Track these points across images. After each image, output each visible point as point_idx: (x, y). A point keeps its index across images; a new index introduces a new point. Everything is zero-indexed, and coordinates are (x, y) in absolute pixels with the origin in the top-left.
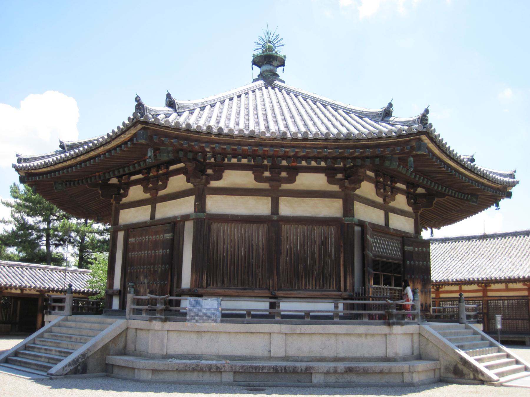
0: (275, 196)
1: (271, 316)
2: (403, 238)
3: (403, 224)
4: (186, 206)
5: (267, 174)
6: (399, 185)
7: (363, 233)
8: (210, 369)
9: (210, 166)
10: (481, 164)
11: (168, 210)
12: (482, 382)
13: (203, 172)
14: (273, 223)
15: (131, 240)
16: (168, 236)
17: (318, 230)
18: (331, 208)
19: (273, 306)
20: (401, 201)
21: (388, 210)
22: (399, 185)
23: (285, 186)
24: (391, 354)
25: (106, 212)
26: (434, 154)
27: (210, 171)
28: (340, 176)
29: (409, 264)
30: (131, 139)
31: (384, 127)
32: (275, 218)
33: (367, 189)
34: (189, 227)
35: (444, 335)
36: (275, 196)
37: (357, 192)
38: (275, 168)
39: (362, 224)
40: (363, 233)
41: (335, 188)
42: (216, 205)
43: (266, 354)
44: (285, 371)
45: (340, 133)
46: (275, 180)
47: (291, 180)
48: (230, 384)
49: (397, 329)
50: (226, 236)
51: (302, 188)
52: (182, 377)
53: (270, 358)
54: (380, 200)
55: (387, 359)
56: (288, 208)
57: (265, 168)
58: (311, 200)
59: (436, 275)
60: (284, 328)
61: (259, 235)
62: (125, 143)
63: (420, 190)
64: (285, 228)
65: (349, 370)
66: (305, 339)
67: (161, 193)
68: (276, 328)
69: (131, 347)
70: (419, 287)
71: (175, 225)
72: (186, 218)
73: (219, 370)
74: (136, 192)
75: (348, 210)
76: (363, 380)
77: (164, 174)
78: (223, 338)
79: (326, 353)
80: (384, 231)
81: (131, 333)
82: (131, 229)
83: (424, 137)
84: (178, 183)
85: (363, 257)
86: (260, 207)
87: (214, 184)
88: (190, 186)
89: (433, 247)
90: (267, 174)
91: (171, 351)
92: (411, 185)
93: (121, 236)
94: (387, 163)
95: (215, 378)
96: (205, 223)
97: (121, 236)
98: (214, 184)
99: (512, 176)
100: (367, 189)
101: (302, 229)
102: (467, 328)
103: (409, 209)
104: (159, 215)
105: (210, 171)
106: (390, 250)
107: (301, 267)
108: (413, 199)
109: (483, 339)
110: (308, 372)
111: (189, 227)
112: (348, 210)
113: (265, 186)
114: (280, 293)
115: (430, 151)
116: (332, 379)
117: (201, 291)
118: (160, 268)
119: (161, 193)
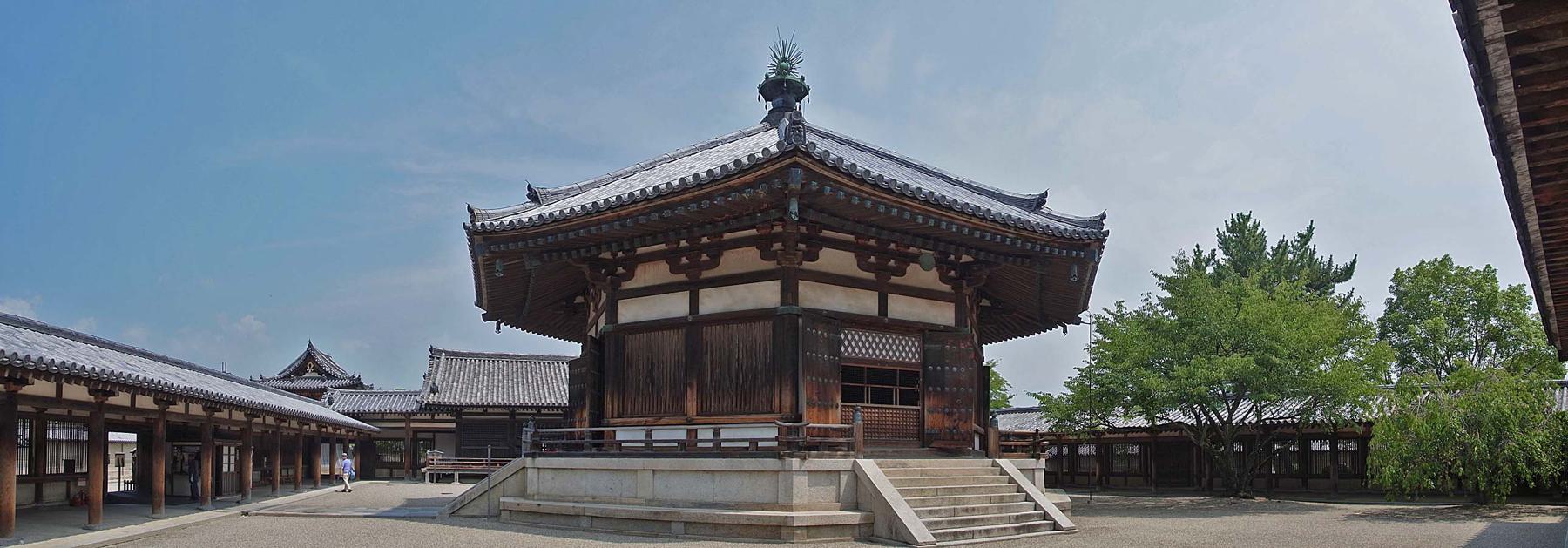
0: (693, 287)
1: (687, 449)
14: (694, 325)
18: (766, 295)
21: (885, 293)
23: (706, 274)
28: (777, 246)
36: (693, 287)
41: (770, 265)
46: (697, 266)
47: (714, 262)
54: (870, 276)
56: (714, 301)
80: (880, 324)
101: (738, 330)
103: (947, 288)
113: (682, 277)
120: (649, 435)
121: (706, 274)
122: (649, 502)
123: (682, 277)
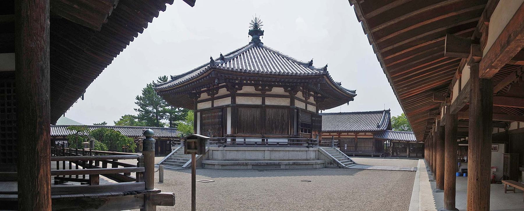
0: (263, 97)
2: (312, 114)
3: (311, 108)
4: (227, 101)
5: (260, 87)
6: (311, 93)
7: (298, 112)
8: (243, 165)
9: (237, 84)
10: (343, 86)
11: (219, 103)
12: (340, 168)
13: (234, 87)
14: (263, 107)
15: (204, 116)
16: (220, 113)
17: (280, 111)
18: (285, 102)
19: (263, 140)
20: (312, 99)
21: (307, 103)
22: (311, 93)
23: (268, 93)
24: (308, 158)
25: (191, 105)
26: (328, 83)
27: (237, 87)
28: (289, 89)
29: (314, 124)
30: (208, 75)
31: (309, 71)
32: (264, 106)
33: (299, 94)
34: (229, 110)
35: (327, 151)
36: (263, 97)
37: (296, 96)
38: (263, 86)
39: (297, 109)
40: (298, 112)
41: (287, 94)
42: (240, 101)
43: (263, 158)
44: (271, 165)
45: (293, 73)
48: (251, 169)
49: (311, 149)
50: (245, 114)
51: (274, 93)
52: (232, 167)
53: (264, 160)
54: (304, 99)
55: (307, 160)
57: (260, 85)
58: (278, 99)
59: (323, 129)
60: (270, 148)
61: (257, 113)
62: (206, 77)
63: (319, 95)
64: (268, 110)
65: (294, 164)
66: (277, 153)
67: (216, 96)
68: (266, 148)
69: (211, 157)
70: (317, 133)
71: (223, 109)
72: (228, 106)
73: (247, 165)
74: (204, 96)
75: (292, 103)
76: (299, 167)
77: (217, 88)
78: (247, 153)
79: (285, 158)
80: (305, 111)
81: (211, 152)
82: (202, 111)
83: (325, 76)
84: (223, 91)
85: (298, 122)
86: (257, 101)
87: (239, 92)
88: (229, 92)
89: (323, 117)
90: (260, 87)
91: (227, 158)
92: (316, 93)
93: (199, 114)
94: (310, 85)
95: (245, 167)
96: (236, 108)
97: (199, 114)
98: (239, 92)
99: (354, 92)
100: (299, 94)
101: (274, 110)
102: (334, 149)
103: (315, 103)
104: (215, 105)
105: (237, 87)
106: (307, 119)
107: (274, 125)
108: (316, 99)
109: (340, 153)
110: (279, 165)
111: (229, 110)
112: (292, 103)
113: (259, 92)
114: (266, 136)
115: (326, 82)
116: (288, 167)
117: (235, 135)
118: (217, 127)
119: (216, 96)
120: (245, 140)
121: (268, 93)
122: (269, 160)
123: (259, 92)
